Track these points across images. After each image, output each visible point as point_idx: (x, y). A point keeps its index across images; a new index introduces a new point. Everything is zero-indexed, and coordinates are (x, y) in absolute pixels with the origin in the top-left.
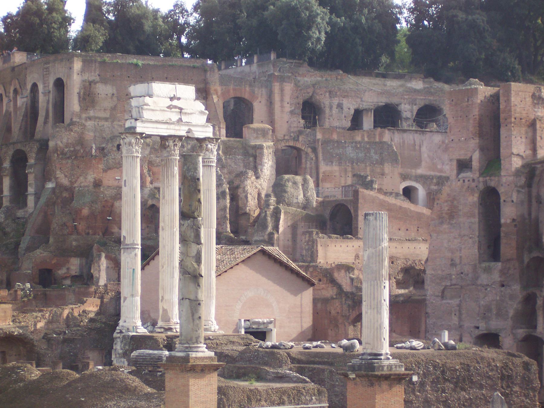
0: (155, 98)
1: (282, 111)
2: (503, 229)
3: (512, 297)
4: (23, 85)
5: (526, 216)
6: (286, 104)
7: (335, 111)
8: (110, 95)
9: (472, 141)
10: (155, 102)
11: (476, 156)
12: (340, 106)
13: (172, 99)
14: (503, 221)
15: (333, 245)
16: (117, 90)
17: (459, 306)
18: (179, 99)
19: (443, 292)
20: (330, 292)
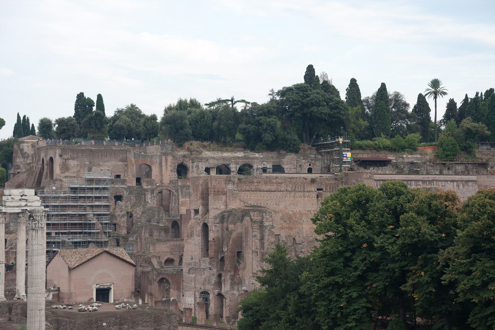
0: (12, 197)
1: (166, 170)
2: (209, 243)
3: (213, 275)
4: (39, 159)
5: (221, 237)
6: (168, 167)
7: (195, 169)
8: (76, 165)
9: (199, 201)
10: (12, 198)
11: (201, 209)
12: (197, 166)
13: (22, 196)
14: (209, 239)
15: (159, 244)
16: (80, 163)
17: (195, 278)
18: (26, 196)
19: (189, 270)
20: (149, 269)
